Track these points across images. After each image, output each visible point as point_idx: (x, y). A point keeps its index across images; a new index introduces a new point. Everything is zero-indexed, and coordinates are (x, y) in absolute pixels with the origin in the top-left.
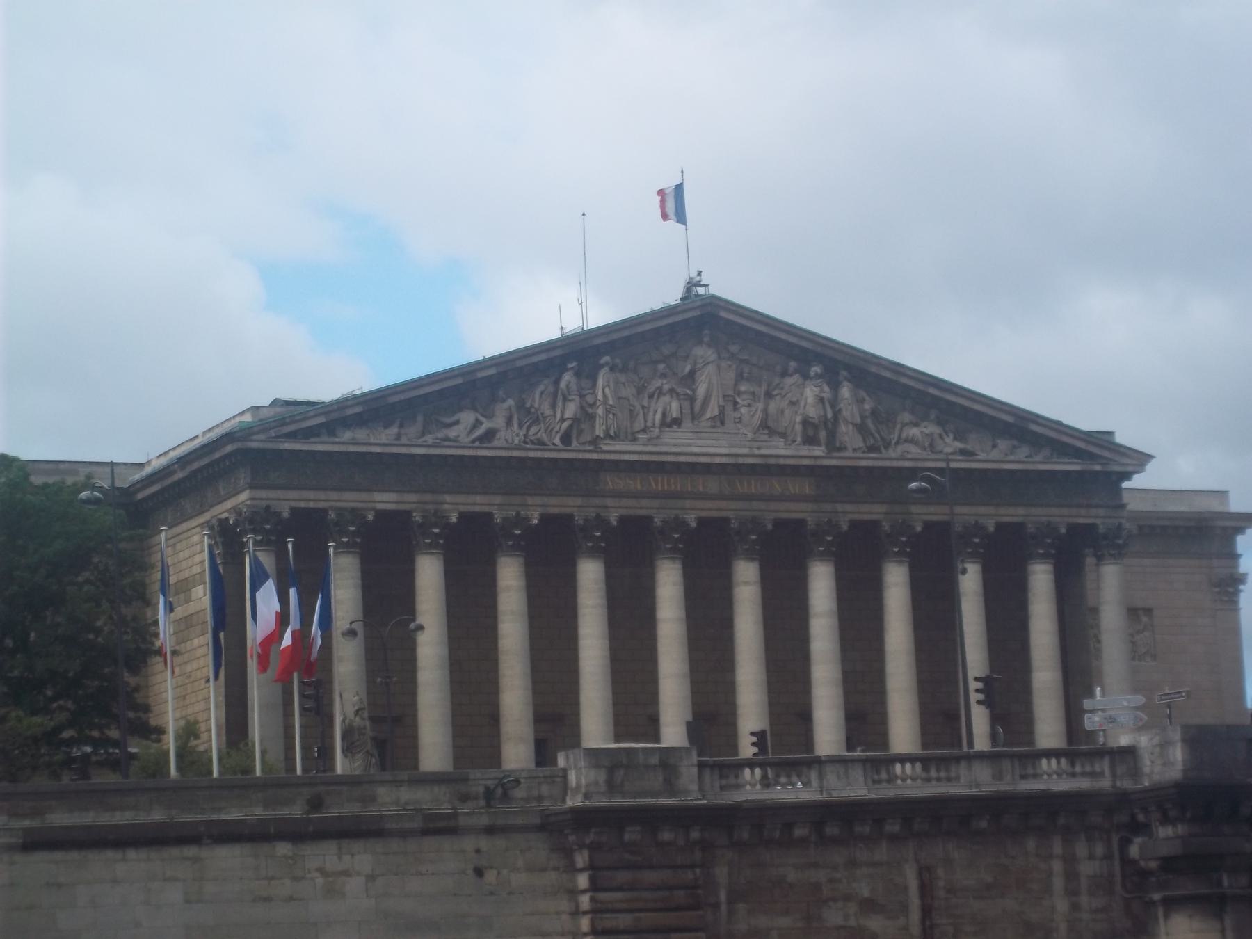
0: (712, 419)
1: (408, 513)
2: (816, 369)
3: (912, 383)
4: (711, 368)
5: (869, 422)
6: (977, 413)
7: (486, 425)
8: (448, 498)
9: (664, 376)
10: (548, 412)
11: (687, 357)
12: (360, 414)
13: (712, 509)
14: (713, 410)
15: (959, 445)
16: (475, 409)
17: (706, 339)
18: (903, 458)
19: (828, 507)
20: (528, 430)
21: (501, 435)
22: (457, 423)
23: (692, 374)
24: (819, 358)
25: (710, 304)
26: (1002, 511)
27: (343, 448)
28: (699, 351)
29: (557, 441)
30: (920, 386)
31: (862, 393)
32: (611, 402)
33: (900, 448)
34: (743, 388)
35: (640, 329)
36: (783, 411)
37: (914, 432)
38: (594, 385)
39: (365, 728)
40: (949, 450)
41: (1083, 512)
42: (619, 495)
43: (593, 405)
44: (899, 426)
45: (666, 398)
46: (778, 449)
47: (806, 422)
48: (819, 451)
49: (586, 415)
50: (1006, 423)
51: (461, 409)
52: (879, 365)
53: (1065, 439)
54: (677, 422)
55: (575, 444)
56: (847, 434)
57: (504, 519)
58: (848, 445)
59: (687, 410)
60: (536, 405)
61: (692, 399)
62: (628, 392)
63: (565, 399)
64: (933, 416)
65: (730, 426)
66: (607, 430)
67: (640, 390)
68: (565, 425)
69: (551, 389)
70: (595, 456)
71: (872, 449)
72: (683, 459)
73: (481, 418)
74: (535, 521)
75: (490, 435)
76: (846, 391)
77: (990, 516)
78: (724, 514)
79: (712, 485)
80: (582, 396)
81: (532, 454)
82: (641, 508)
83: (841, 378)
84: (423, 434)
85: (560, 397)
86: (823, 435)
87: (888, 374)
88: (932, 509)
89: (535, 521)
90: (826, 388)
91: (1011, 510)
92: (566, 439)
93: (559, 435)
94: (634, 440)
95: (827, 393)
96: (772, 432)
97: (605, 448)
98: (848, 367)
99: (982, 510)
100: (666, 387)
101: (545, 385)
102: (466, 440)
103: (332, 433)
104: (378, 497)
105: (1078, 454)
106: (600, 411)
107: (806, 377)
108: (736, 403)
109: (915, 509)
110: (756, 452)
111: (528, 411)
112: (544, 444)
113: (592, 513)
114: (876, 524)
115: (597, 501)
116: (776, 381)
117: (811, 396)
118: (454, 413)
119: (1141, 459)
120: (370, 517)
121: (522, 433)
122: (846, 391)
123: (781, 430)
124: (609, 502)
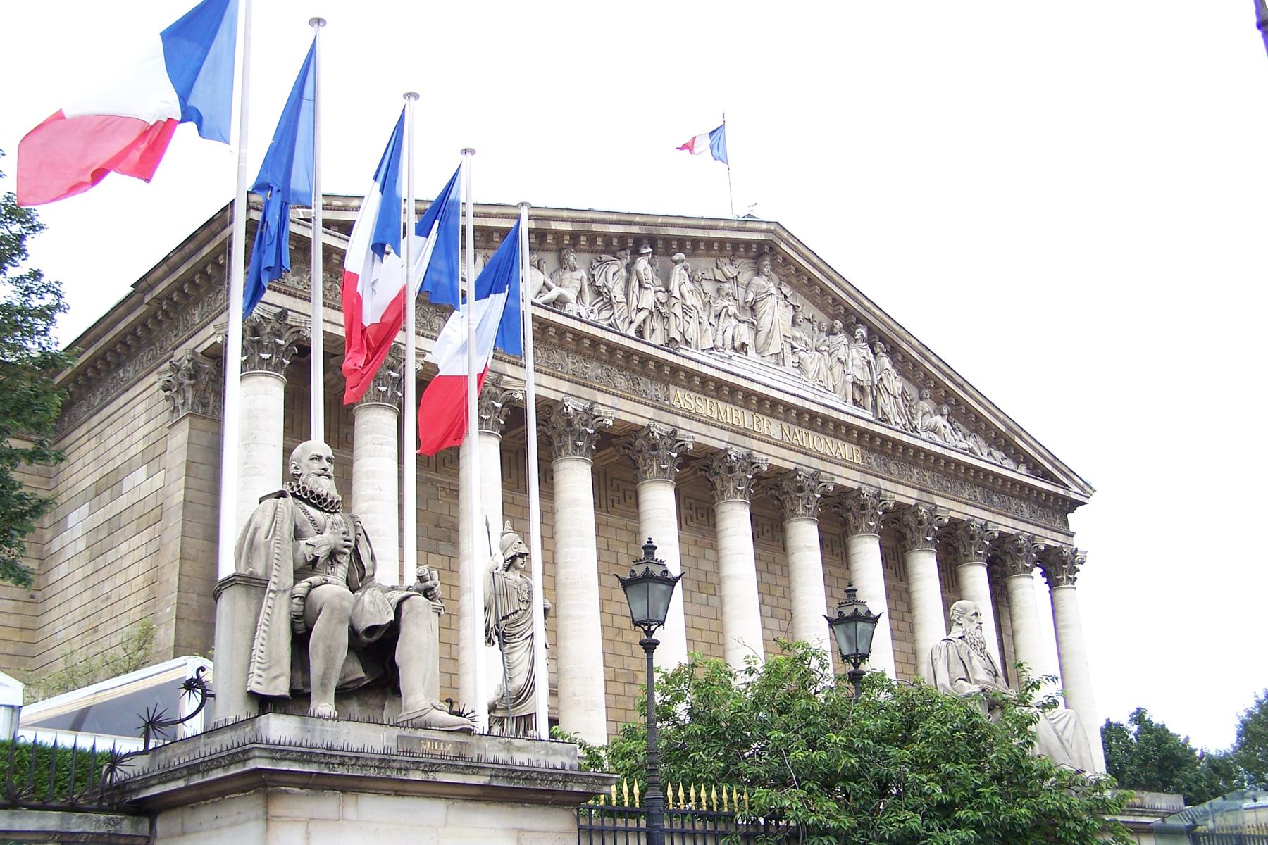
2: (861, 331)
3: (934, 370)
6: (979, 417)
10: (621, 298)
14: (775, 349)
19: (873, 480)
24: (861, 320)
28: (757, 280)
29: (632, 333)
32: (689, 303)
34: (798, 335)
36: (831, 369)
40: (965, 446)
42: (691, 417)
44: (920, 414)
47: (854, 383)
49: (660, 313)
52: (909, 343)
56: (889, 406)
58: (891, 416)
60: (610, 285)
61: (755, 328)
63: (641, 286)
66: (683, 334)
69: (624, 272)
73: (549, 282)
75: (558, 304)
79: (774, 428)
82: (716, 439)
83: (877, 350)
85: (635, 283)
86: (870, 399)
87: (916, 356)
89: (610, 422)
92: (640, 332)
93: (634, 326)
97: (682, 352)
101: (618, 267)
106: (678, 310)
108: (793, 348)
109: (938, 501)
110: (819, 400)
114: (913, 510)
115: (667, 417)
116: (825, 338)
122: (886, 362)
124: (681, 422)
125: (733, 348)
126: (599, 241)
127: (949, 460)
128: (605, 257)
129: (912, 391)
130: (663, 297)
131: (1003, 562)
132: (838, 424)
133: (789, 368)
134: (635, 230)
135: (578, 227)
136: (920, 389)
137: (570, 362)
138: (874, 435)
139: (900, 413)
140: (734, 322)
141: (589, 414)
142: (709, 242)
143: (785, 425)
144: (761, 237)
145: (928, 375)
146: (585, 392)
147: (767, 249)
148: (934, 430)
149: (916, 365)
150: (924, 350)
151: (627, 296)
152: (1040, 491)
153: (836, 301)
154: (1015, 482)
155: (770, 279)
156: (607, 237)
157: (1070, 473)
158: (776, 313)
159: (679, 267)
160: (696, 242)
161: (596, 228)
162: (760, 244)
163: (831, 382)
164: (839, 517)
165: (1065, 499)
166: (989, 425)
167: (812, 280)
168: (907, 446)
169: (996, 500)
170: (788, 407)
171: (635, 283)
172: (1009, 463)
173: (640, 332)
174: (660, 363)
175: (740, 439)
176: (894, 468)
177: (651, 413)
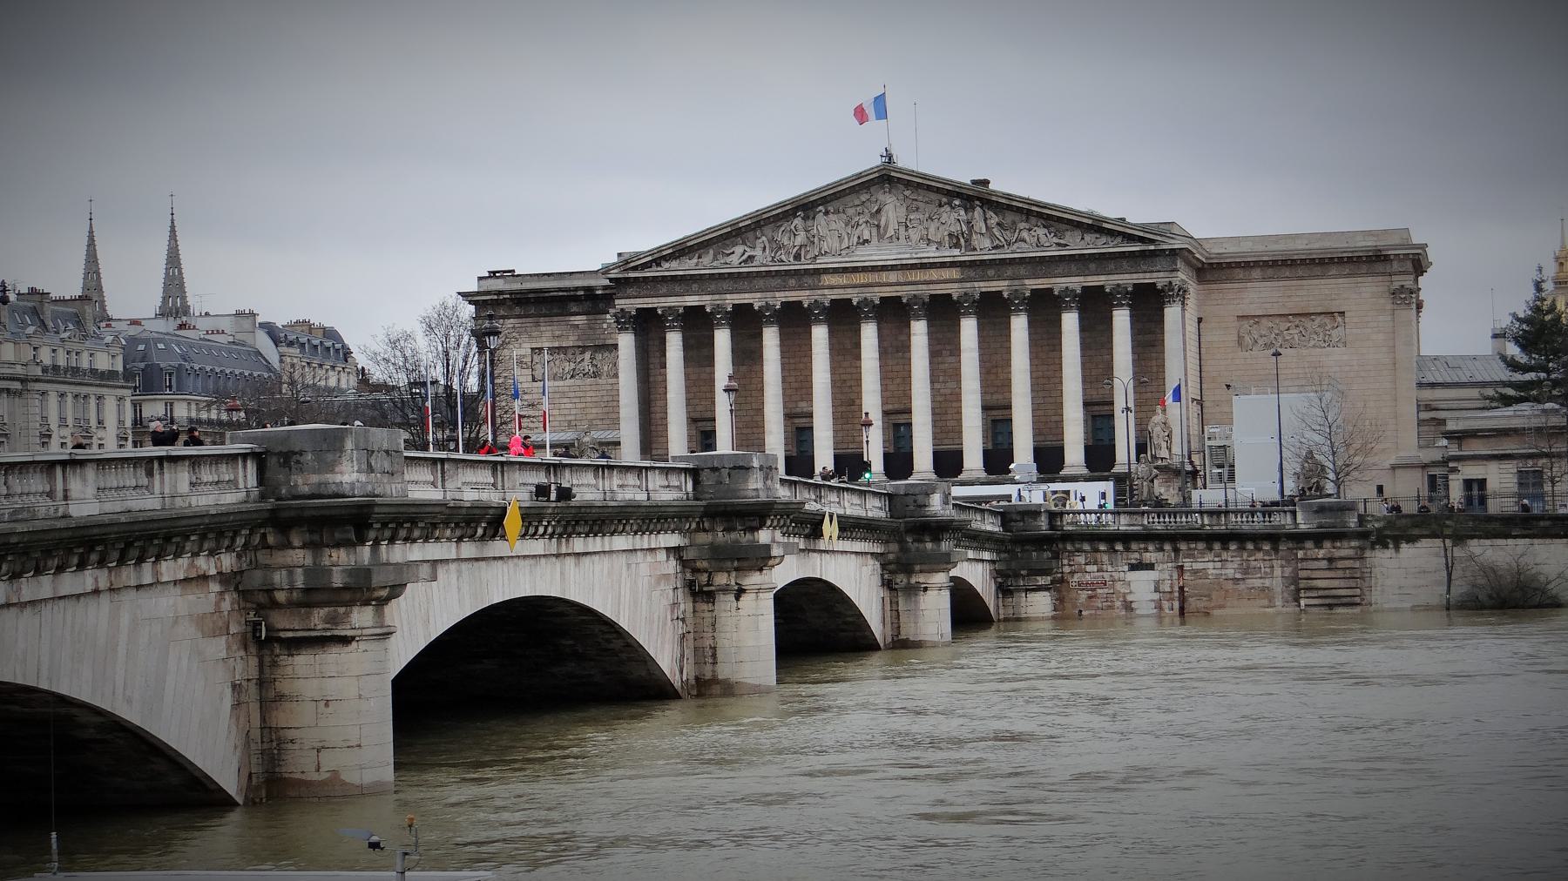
5: (996, 231)
13: (888, 292)
15: (1056, 240)
16: (744, 243)
23: (879, 211)
24: (959, 195)
28: (881, 197)
31: (990, 214)
42: (832, 288)
46: (931, 253)
48: (956, 252)
56: (976, 241)
61: (878, 226)
75: (751, 258)
76: (978, 212)
77: (1075, 282)
79: (893, 277)
90: (962, 212)
91: (1095, 278)
92: (797, 257)
98: (978, 199)
103: (659, 265)
104: (687, 298)
105: (1142, 240)
117: (952, 218)
122: (978, 212)
129: (1017, 217)
137: (760, 283)
139: (992, 236)
146: (769, 294)
148: (1024, 241)
150: (1009, 197)
164: (943, 312)
169: (1092, 266)
172: (1104, 239)
173: (797, 257)
176: (991, 272)
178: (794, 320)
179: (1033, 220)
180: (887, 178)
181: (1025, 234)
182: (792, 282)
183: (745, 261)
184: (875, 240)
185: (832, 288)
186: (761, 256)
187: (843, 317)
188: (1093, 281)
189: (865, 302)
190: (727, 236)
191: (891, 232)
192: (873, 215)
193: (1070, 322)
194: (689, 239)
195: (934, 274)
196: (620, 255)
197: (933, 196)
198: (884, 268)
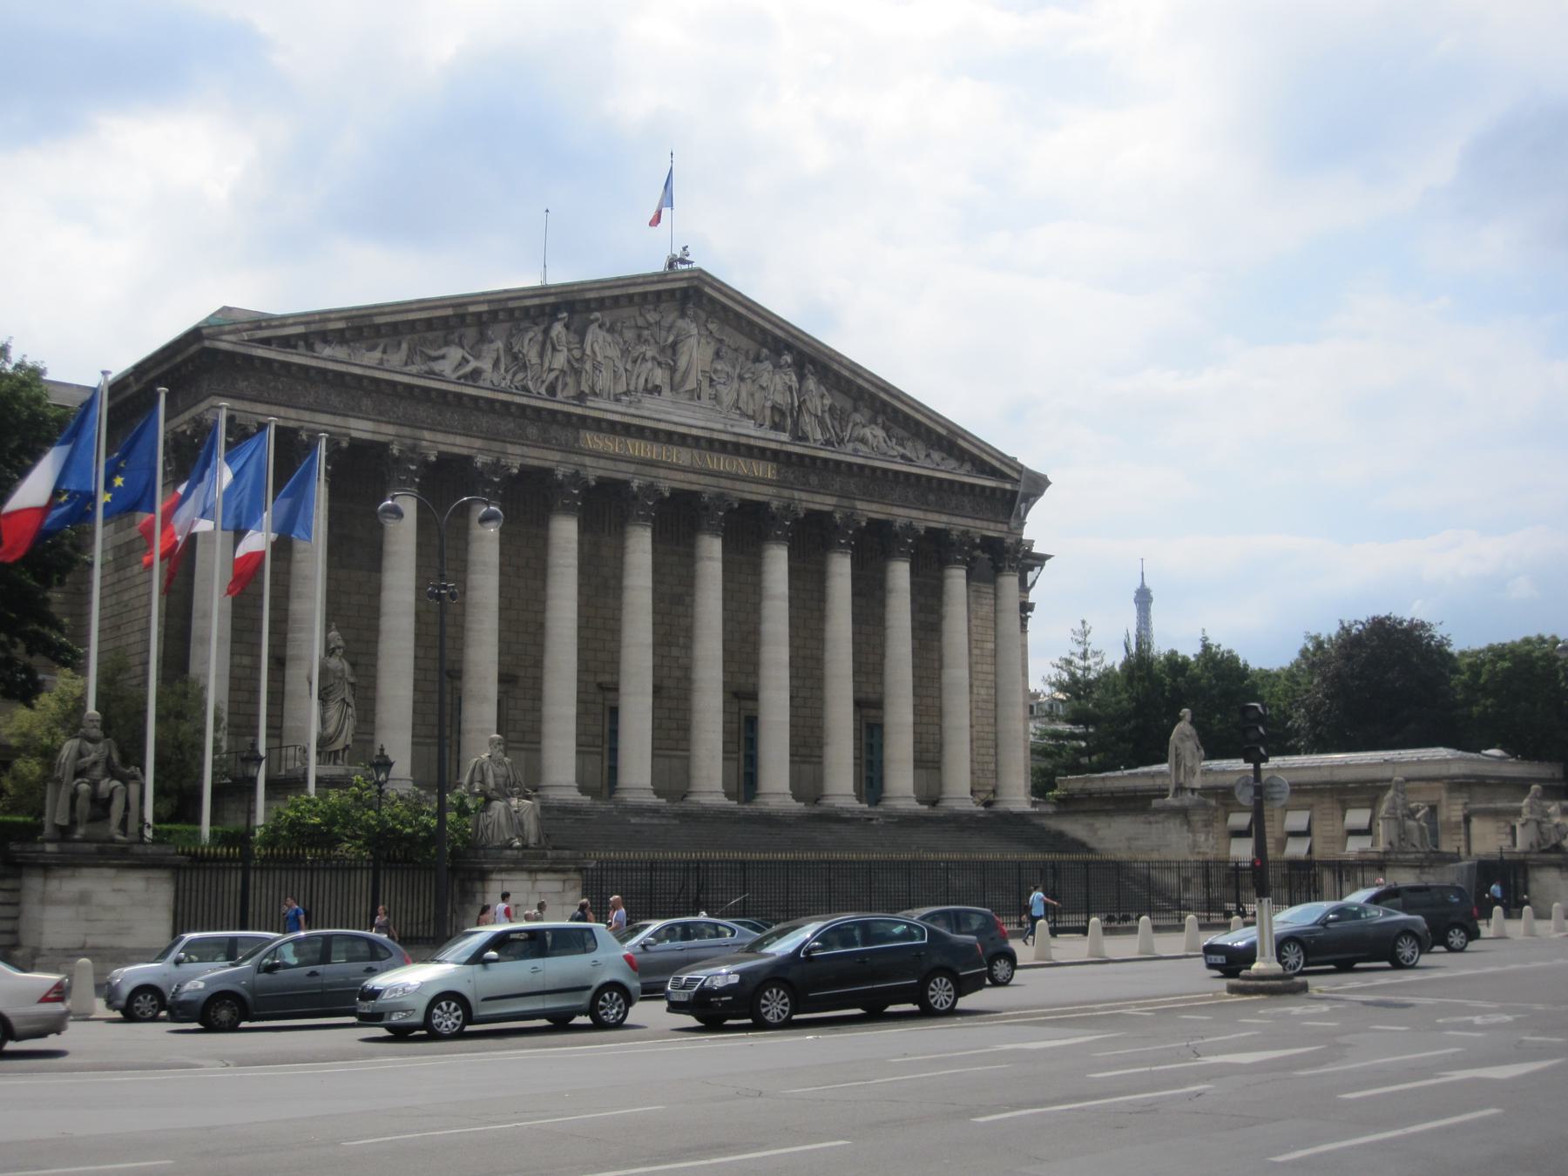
0: (692, 391)
1: (385, 446)
3: (866, 385)
4: (693, 341)
5: (827, 415)
6: (918, 423)
7: (473, 364)
8: (427, 435)
9: (646, 341)
11: (670, 329)
12: (342, 331)
14: (691, 384)
17: (690, 312)
18: (855, 453)
19: (786, 493)
20: (515, 374)
21: (485, 375)
22: (443, 357)
23: (674, 345)
24: (789, 347)
25: (697, 278)
26: (930, 516)
27: (321, 364)
28: (680, 323)
29: (543, 391)
30: (873, 389)
31: (823, 389)
33: (850, 447)
35: (632, 290)
37: (867, 432)
38: (582, 342)
39: (343, 671)
41: (992, 525)
43: (581, 360)
45: (649, 364)
46: (748, 430)
47: (773, 408)
48: (785, 437)
50: (939, 436)
51: (447, 343)
52: (840, 363)
53: (985, 457)
54: (657, 389)
55: (560, 396)
57: (484, 464)
59: (667, 380)
61: (673, 370)
62: (614, 352)
63: (554, 349)
64: (880, 421)
65: (706, 401)
66: (592, 388)
67: (625, 353)
68: (553, 375)
69: (540, 337)
70: (579, 411)
71: (828, 442)
72: (662, 426)
74: (515, 471)
75: (476, 374)
78: (695, 488)
79: (682, 456)
80: (569, 350)
81: (518, 400)
82: (621, 472)
84: (406, 364)
85: (549, 346)
86: (789, 420)
87: (846, 373)
88: (874, 507)
91: (936, 517)
92: (552, 390)
94: (618, 400)
95: (793, 380)
96: (744, 415)
98: (813, 361)
99: (914, 513)
100: (649, 354)
101: (535, 333)
102: (453, 377)
105: (994, 473)
106: (588, 366)
107: (777, 366)
108: (711, 380)
109: (859, 505)
111: (515, 357)
112: (528, 390)
113: (570, 470)
114: (830, 514)
115: (576, 458)
116: (749, 364)
117: (777, 383)
118: (440, 347)
119: (1038, 484)
120: (344, 444)
121: (509, 377)
122: (811, 383)
123: (750, 412)
124: (588, 461)
125: (646, 390)
126: (517, 314)
127: (874, 469)
128: (524, 325)
129: (848, 405)
130: (577, 353)
131: (931, 555)
132: (750, 448)
133: (706, 401)
134: (551, 300)
135: (493, 307)
136: (855, 400)
138: (789, 454)
140: (649, 364)
141: (496, 467)
142: (630, 297)
143: (695, 452)
144: (683, 284)
145: (860, 388)
146: (496, 446)
147: (691, 292)
148: (863, 441)
149: (849, 381)
150: (855, 369)
151: (541, 355)
152: (983, 488)
153: (763, 331)
154: (951, 482)
155: (695, 319)
156: (526, 309)
157: (1021, 469)
158: (696, 353)
159: (594, 327)
160: (616, 299)
161: (511, 304)
162: (685, 290)
163: (751, 407)
164: (747, 528)
165: (1014, 493)
166: (929, 430)
167: (738, 315)
168: (826, 461)
169: (932, 497)
170: (697, 439)
171: (549, 346)
172: (952, 463)
173: (552, 390)
174: (569, 415)
175: (647, 470)
176: (814, 480)
177: (558, 456)
178: (528, 501)
179: (867, 413)
180: (689, 296)
181: (867, 432)
182: (532, 431)
183: (465, 377)
184: (666, 392)
185: (598, 455)
186: (486, 371)
187: (606, 508)
188: (938, 520)
189: (651, 489)
190: (429, 324)
191: (691, 384)
192: (662, 350)
193: (900, 574)
194: (380, 310)
195: (741, 465)
196: (226, 310)
197: (744, 343)
198: (681, 440)
